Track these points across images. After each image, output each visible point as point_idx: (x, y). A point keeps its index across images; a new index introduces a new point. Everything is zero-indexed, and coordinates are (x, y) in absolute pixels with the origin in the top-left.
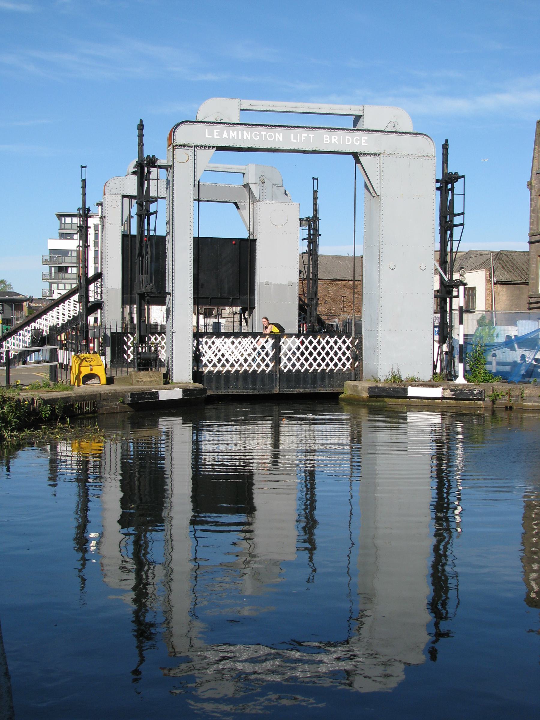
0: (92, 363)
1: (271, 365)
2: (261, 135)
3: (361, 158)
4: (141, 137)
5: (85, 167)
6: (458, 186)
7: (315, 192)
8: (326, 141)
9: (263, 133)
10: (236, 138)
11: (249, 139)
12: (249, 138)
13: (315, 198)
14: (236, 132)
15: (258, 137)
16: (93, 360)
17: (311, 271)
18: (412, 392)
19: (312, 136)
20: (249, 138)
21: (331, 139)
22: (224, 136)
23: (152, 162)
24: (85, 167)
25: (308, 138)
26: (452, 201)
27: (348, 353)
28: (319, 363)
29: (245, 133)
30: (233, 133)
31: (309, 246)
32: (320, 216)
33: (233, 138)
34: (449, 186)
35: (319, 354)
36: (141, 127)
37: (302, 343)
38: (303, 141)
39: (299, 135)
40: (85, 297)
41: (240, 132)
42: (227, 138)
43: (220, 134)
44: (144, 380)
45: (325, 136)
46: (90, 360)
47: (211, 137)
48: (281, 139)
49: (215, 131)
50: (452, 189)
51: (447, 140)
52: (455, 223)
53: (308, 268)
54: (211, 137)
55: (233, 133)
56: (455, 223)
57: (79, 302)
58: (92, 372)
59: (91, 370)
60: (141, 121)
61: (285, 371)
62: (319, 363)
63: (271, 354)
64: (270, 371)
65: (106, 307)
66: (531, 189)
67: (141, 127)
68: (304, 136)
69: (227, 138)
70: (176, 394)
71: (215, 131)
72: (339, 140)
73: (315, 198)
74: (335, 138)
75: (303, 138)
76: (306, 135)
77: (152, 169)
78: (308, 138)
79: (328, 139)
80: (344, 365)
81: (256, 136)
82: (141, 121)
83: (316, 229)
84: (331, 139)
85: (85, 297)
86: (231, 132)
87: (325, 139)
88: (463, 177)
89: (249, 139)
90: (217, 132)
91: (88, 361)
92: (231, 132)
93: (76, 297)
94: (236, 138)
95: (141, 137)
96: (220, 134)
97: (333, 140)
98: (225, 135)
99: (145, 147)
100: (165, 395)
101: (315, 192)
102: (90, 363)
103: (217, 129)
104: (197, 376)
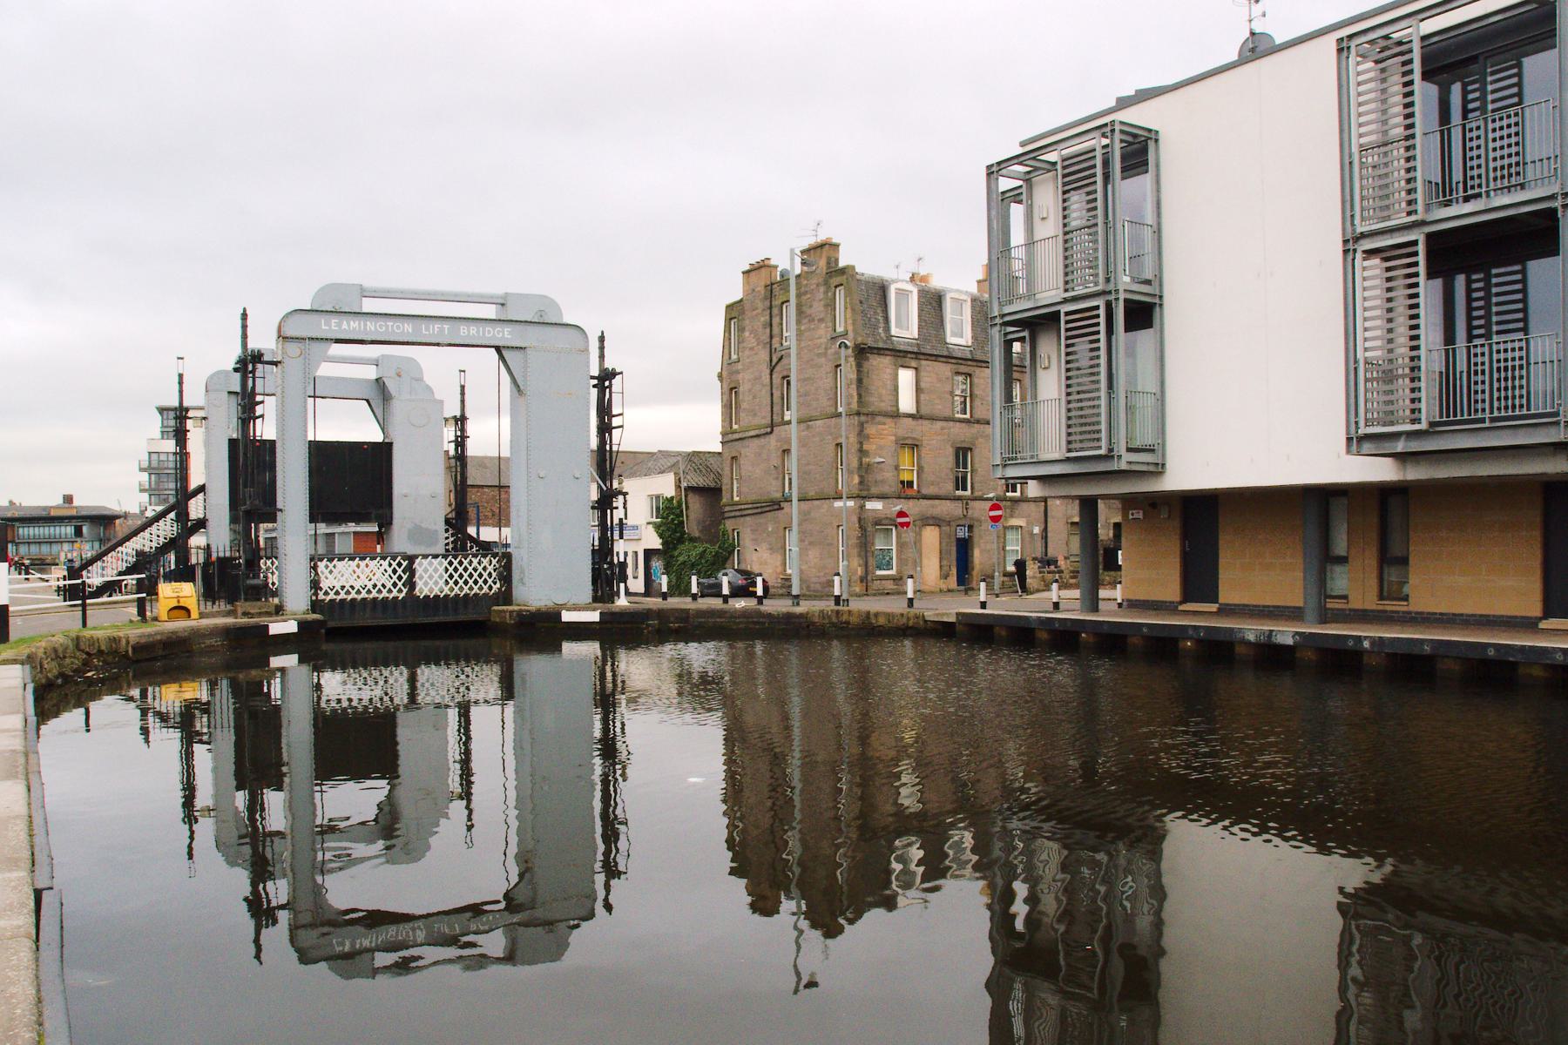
1: (405, 591)
3: (505, 353)
4: (244, 327)
5: (182, 358)
6: (616, 381)
7: (463, 387)
12: (373, 329)
13: (463, 394)
14: (357, 323)
17: (459, 478)
18: (567, 617)
20: (373, 329)
21: (469, 331)
23: (257, 357)
24: (182, 358)
25: (441, 330)
26: (610, 400)
27: (494, 575)
28: (461, 587)
31: (456, 449)
32: (467, 415)
34: (607, 383)
35: (461, 576)
36: (244, 316)
37: (451, 563)
40: (183, 516)
43: (339, 325)
48: (410, 330)
50: (610, 387)
51: (603, 333)
52: (614, 425)
53: (456, 475)
56: (614, 425)
57: (177, 521)
60: (245, 310)
62: (461, 587)
63: (405, 577)
65: (210, 524)
66: (721, 381)
67: (244, 316)
70: (291, 627)
72: (478, 332)
73: (463, 394)
77: (259, 366)
78: (441, 330)
80: (490, 588)
81: (381, 326)
82: (245, 310)
83: (463, 430)
85: (183, 516)
86: (352, 323)
88: (621, 373)
92: (352, 323)
93: (172, 515)
95: (244, 327)
96: (339, 325)
98: (345, 326)
99: (249, 339)
100: (277, 628)
101: (463, 387)
103: (334, 321)
104: (316, 606)
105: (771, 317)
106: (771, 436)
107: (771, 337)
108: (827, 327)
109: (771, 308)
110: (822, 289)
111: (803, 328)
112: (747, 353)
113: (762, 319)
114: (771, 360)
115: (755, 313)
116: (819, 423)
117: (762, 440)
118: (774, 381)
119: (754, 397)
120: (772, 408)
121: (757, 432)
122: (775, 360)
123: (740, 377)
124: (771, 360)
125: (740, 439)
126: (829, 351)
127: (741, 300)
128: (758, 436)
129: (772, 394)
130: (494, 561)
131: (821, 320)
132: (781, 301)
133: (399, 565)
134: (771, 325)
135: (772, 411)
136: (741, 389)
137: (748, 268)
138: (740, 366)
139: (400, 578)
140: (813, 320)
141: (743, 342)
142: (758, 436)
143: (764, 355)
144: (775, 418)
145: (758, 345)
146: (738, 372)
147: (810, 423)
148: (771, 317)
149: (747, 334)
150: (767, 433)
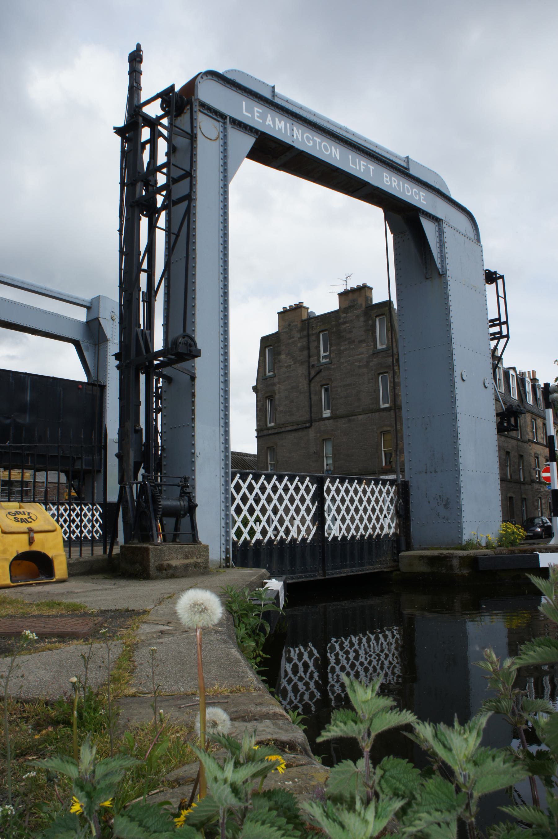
0: (34, 525)
2: (315, 142)
8: (387, 181)
9: (318, 140)
10: (283, 132)
11: (300, 140)
15: (311, 142)
16: (34, 518)
19: (372, 168)
21: (391, 180)
22: (267, 123)
29: (295, 129)
30: (280, 123)
33: (280, 130)
38: (362, 171)
39: (357, 160)
41: (288, 125)
42: (272, 126)
44: (174, 563)
45: (385, 174)
46: (27, 516)
47: (250, 115)
49: (256, 109)
54: (250, 115)
55: (280, 123)
58: (36, 547)
59: (31, 541)
60: (139, 46)
61: (330, 539)
64: (312, 539)
68: (363, 165)
69: (272, 126)
71: (256, 109)
74: (395, 181)
75: (362, 167)
76: (365, 164)
78: (367, 169)
79: (388, 179)
82: (139, 46)
84: (391, 180)
86: (277, 119)
87: (385, 179)
89: (300, 140)
90: (258, 112)
91: (22, 521)
92: (277, 119)
94: (283, 132)
97: (393, 183)
98: (269, 121)
102: (29, 525)
105: (309, 342)
106: (310, 430)
107: (309, 357)
108: (367, 346)
109: (308, 336)
110: (362, 319)
111: (342, 348)
112: (283, 369)
113: (299, 345)
114: (309, 373)
115: (291, 341)
116: (360, 417)
117: (301, 434)
118: (312, 389)
119: (292, 402)
120: (311, 408)
121: (295, 427)
122: (313, 373)
123: (277, 388)
124: (309, 373)
125: (277, 433)
126: (371, 364)
127: (277, 333)
128: (295, 430)
129: (311, 399)
130: (392, 491)
131: (361, 342)
132: (318, 331)
133: (307, 490)
134: (309, 348)
135: (311, 411)
136: (277, 397)
137: (282, 310)
138: (276, 380)
139: (308, 510)
140: (354, 341)
141: (279, 362)
142: (295, 430)
143: (301, 370)
144: (313, 415)
145: (295, 363)
146: (274, 384)
147: (350, 418)
148: (309, 342)
149: (283, 357)
150: (306, 428)
